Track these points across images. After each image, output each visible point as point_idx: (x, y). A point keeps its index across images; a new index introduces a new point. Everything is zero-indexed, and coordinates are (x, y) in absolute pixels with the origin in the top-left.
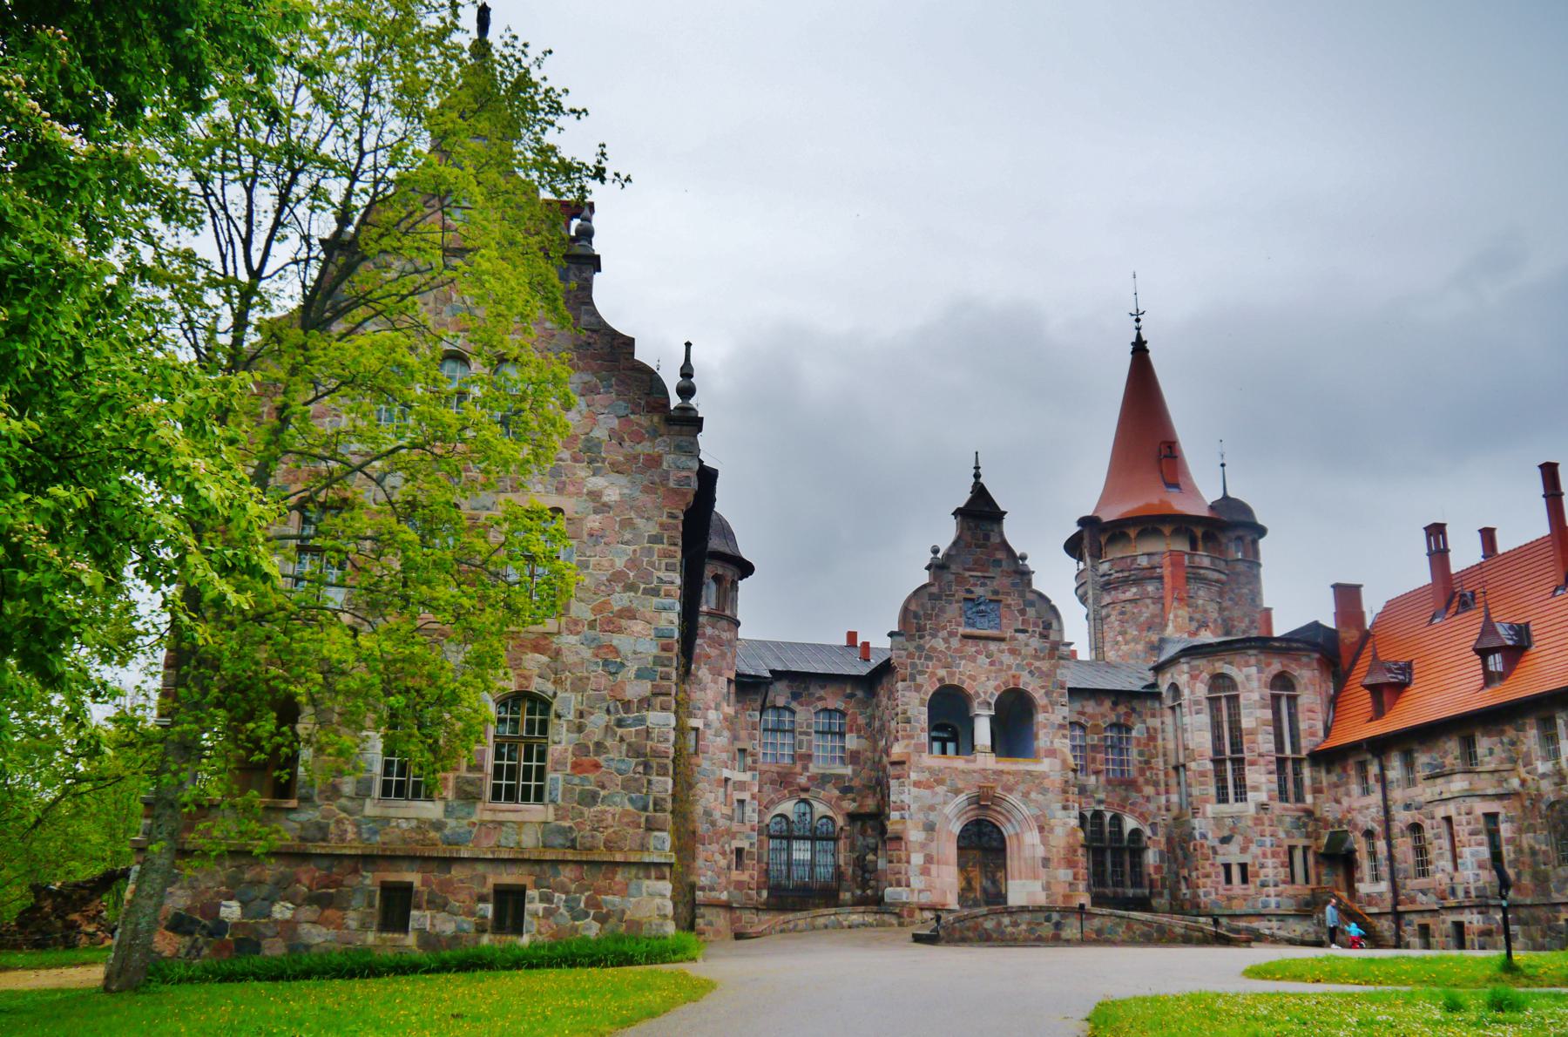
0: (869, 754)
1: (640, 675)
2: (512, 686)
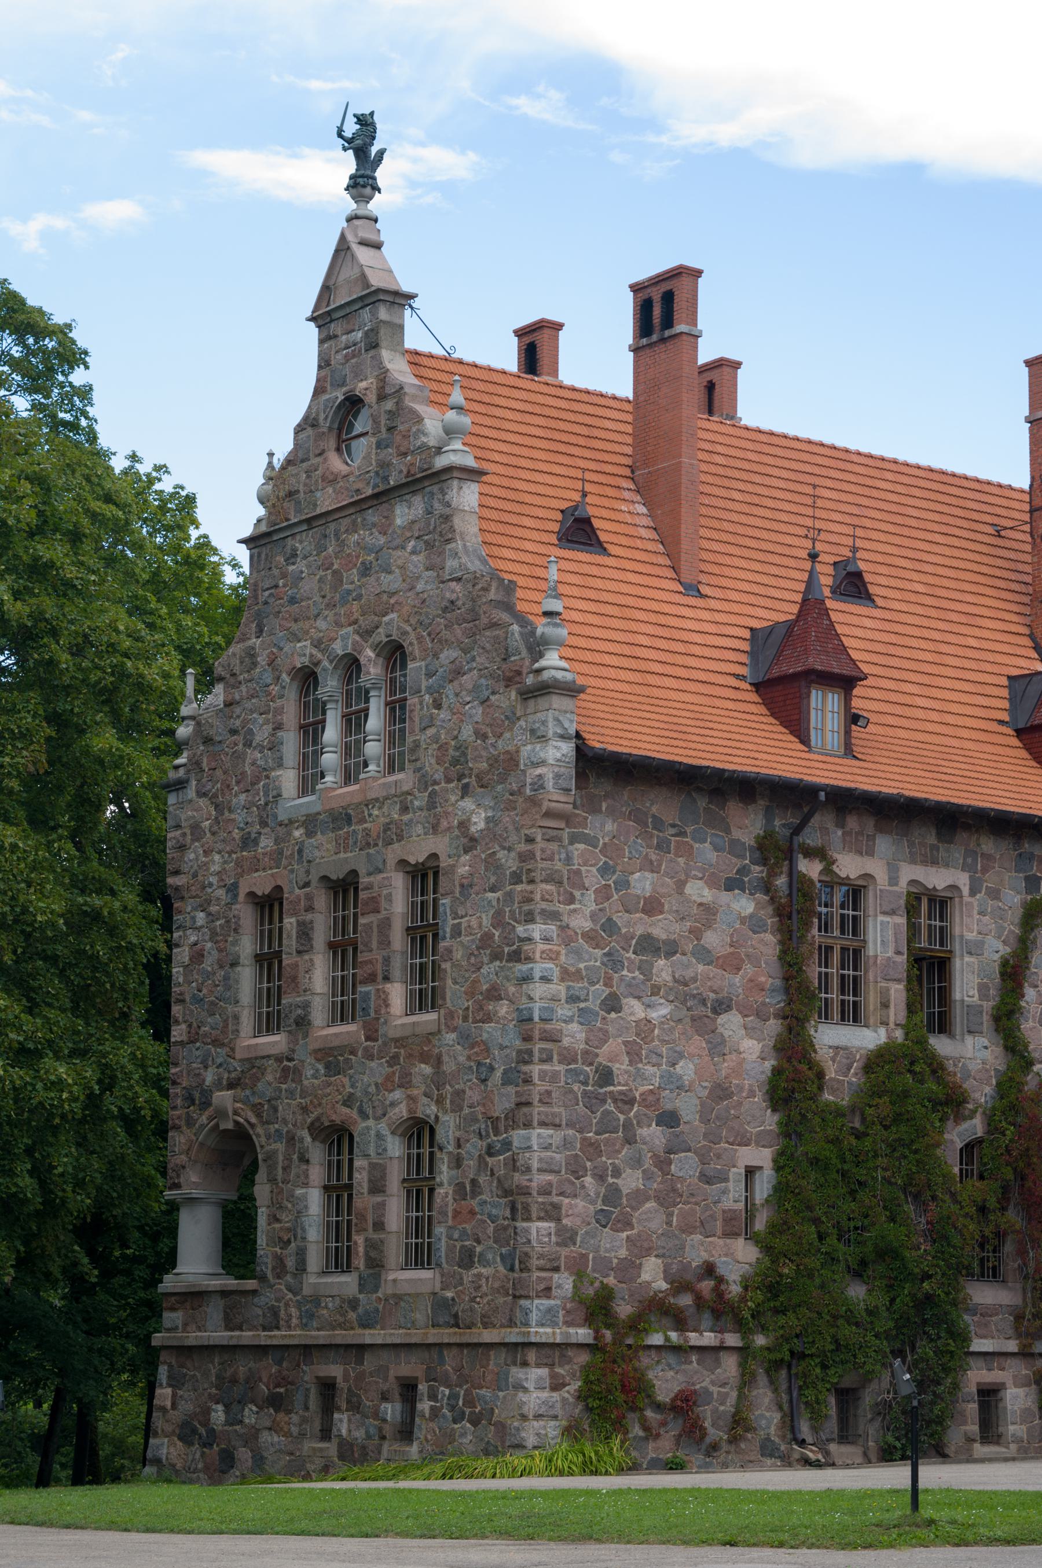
1: (506, 1081)
2: (402, 1111)
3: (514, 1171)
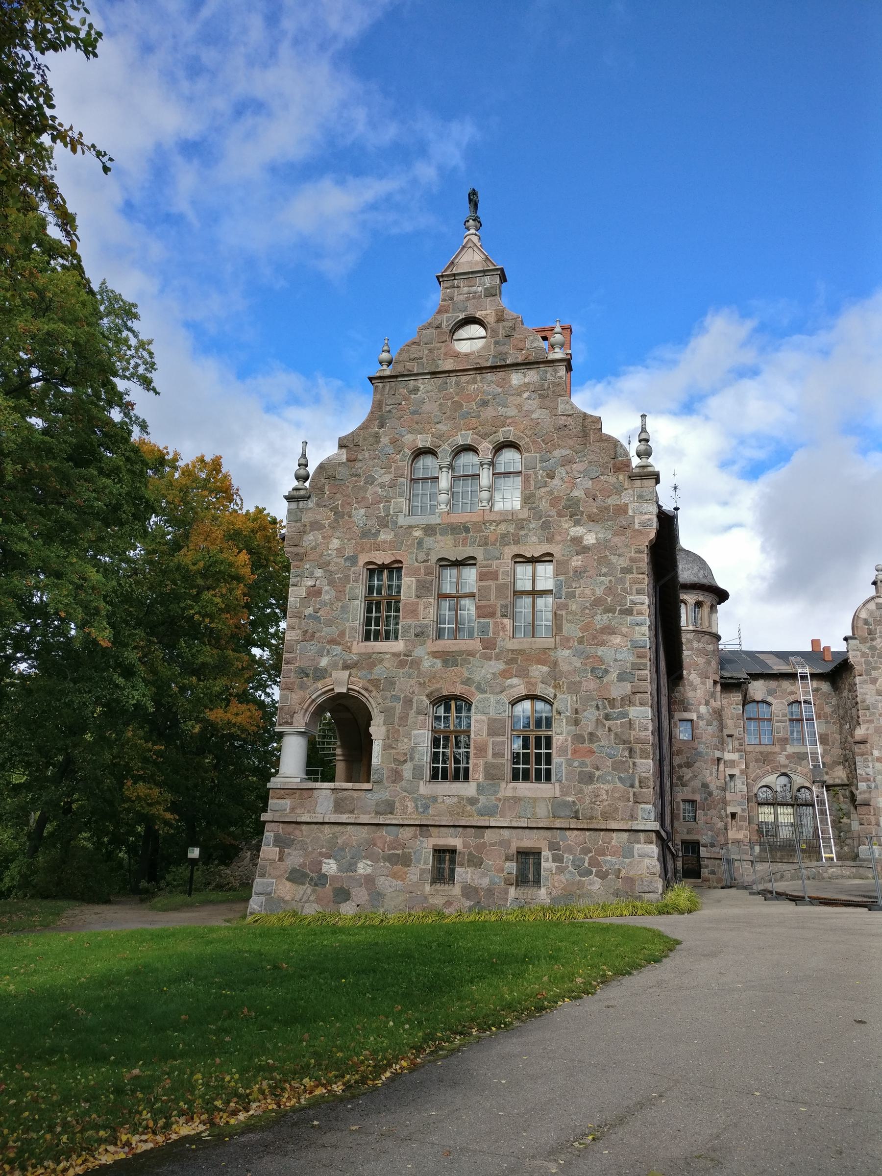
0: (838, 736)
1: (621, 678)
3: (630, 730)
